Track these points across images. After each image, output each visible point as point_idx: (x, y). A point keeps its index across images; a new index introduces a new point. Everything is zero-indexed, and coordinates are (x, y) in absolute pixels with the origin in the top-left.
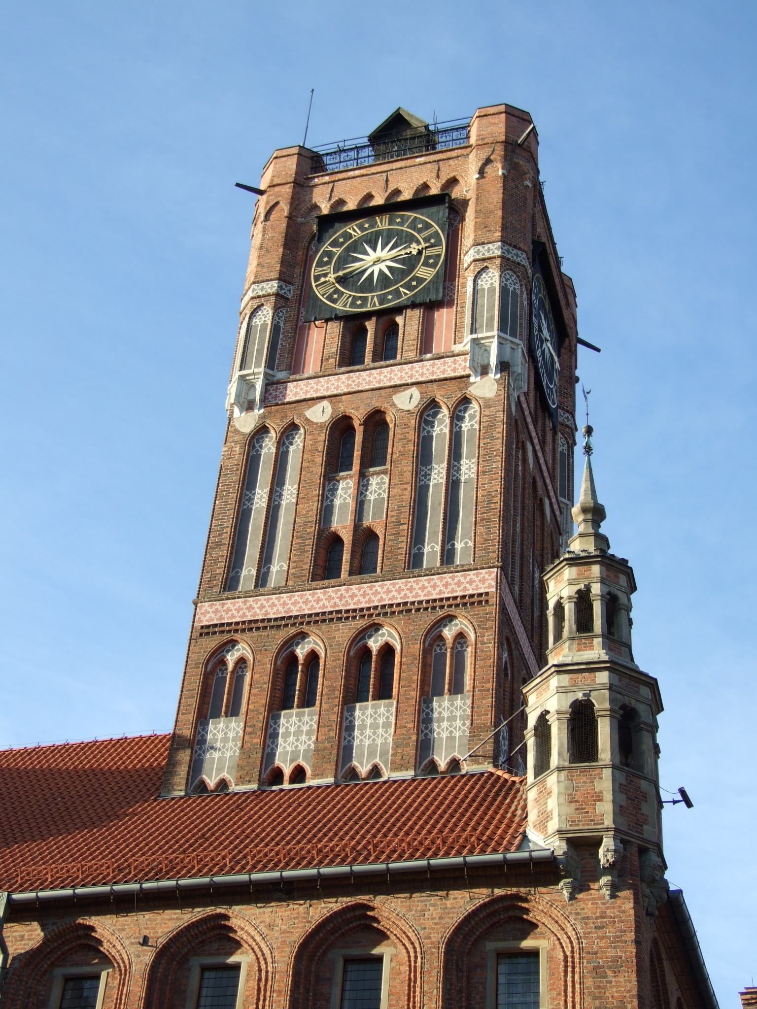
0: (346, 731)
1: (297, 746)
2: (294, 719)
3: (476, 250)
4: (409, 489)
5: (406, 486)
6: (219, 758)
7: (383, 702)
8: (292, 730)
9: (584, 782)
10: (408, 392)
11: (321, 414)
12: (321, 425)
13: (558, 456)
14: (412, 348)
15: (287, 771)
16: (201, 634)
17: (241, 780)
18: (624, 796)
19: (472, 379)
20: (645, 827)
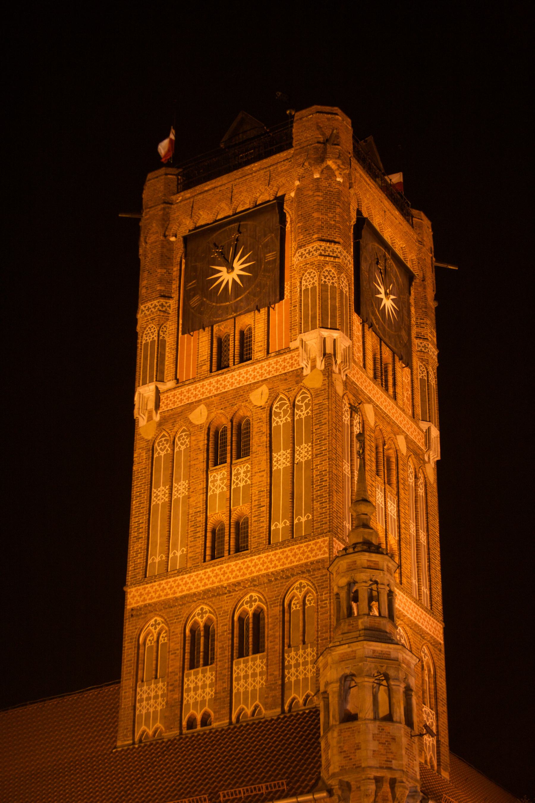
0: (235, 681)
1: (204, 697)
2: (200, 676)
3: (300, 254)
4: (265, 476)
5: (263, 473)
6: (153, 712)
7: (258, 655)
8: (200, 684)
9: (349, 736)
10: (260, 389)
11: (200, 416)
12: (201, 427)
13: (417, 385)
14: (260, 349)
15: (199, 717)
16: (132, 616)
17: (169, 728)
18: (377, 742)
19: (305, 373)
20: (394, 762)
